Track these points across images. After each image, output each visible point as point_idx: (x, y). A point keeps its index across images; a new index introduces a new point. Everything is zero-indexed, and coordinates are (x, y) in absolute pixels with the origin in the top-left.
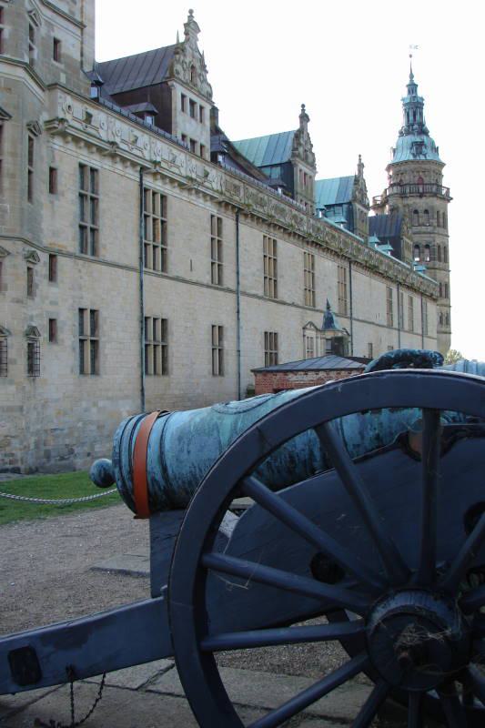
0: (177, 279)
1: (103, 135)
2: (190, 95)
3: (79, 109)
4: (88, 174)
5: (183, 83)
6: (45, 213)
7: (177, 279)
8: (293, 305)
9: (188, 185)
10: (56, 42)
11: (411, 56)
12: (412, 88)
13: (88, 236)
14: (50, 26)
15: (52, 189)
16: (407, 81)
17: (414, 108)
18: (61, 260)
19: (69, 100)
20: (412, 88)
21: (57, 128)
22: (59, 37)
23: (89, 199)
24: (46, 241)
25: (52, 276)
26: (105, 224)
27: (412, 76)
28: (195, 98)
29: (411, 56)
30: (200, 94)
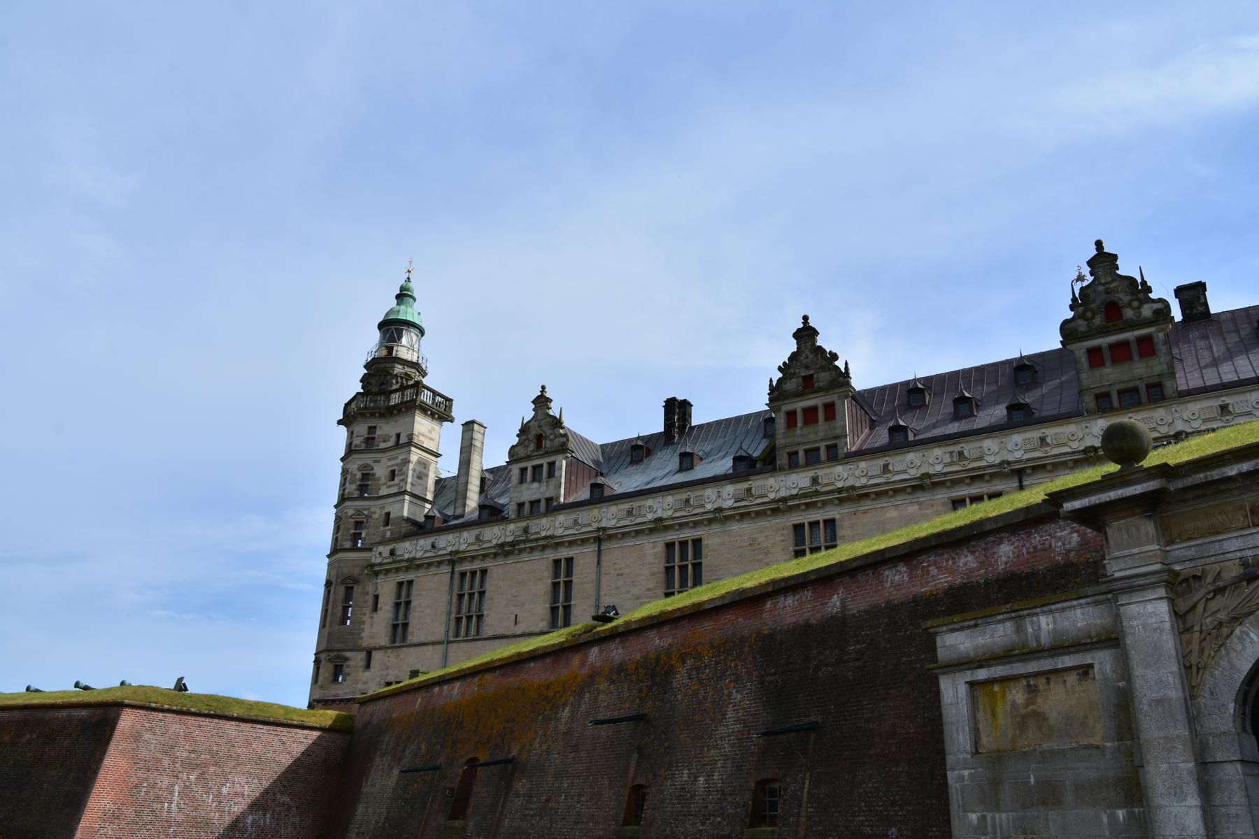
0: (495, 637)
2: (529, 465)
6: (366, 627)
7: (495, 637)
9: (506, 550)
10: (388, 514)
13: (399, 630)
14: (383, 508)
15: (375, 609)
18: (374, 653)
19: (381, 549)
23: (403, 605)
24: (365, 644)
26: (415, 619)
30: (547, 454)
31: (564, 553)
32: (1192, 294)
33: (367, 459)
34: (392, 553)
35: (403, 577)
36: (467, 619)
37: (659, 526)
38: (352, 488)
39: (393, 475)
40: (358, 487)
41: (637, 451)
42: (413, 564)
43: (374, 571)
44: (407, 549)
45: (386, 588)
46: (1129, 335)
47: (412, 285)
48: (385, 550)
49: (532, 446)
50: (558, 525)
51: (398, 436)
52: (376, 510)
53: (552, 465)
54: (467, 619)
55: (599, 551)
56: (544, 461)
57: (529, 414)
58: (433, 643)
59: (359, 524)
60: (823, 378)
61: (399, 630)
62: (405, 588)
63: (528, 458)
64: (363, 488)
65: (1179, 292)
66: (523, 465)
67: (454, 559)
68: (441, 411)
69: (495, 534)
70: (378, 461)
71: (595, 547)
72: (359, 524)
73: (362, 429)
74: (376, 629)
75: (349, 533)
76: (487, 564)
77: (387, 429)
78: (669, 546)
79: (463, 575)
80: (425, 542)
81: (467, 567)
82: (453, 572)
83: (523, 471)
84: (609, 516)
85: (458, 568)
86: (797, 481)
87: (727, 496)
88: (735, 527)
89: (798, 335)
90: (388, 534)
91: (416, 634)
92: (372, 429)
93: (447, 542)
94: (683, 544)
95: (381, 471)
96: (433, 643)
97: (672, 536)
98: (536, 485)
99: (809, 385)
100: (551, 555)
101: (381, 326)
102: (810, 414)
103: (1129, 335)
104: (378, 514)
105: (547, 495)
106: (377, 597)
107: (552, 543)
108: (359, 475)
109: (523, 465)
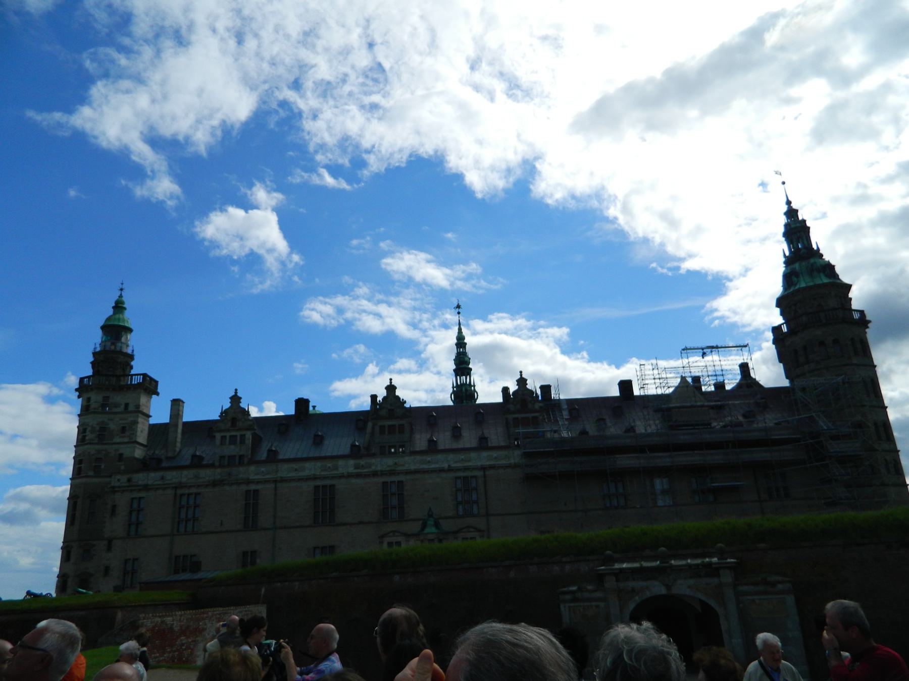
1: (140, 483)
2: (228, 434)
3: (124, 478)
5: (220, 431)
8: (361, 523)
9: (214, 484)
12: (791, 213)
16: (785, 208)
19: (119, 477)
20: (791, 213)
21: (114, 490)
22: (121, 452)
25: (109, 548)
27: (789, 203)
28: (233, 433)
29: (784, 183)
31: (253, 487)
32: (546, 389)
34: (129, 480)
37: (315, 478)
39: (123, 430)
42: (146, 488)
43: (114, 490)
44: (141, 478)
45: (122, 500)
46: (530, 415)
47: (124, 299)
49: (229, 424)
50: (251, 472)
51: (127, 405)
53: (243, 436)
55: (276, 489)
56: (238, 434)
57: (227, 405)
58: (162, 536)
63: (228, 430)
65: (542, 387)
66: (223, 434)
70: (111, 420)
71: (273, 485)
78: (317, 487)
79: (181, 495)
81: (187, 491)
82: (176, 494)
83: (223, 438)
84: (285, 471)
85: (179, 492)
86: (388, 462)
87: (349, 466)
88: (354, 481)
89: (388, 388)
90: (123, 467)
92: (106, 398)
94: (324, 487)
96: (162, 536)
97: (318, 483)
98: (232, 447)
99: (391, 415)
100: (244, 488)
101: (103, 328)
102: (392, 427)
103: (530, 415)
105: (241, 453)
106: (114, 507)
107: (248, 482)
108: (98, 428)
109: (223, 434)
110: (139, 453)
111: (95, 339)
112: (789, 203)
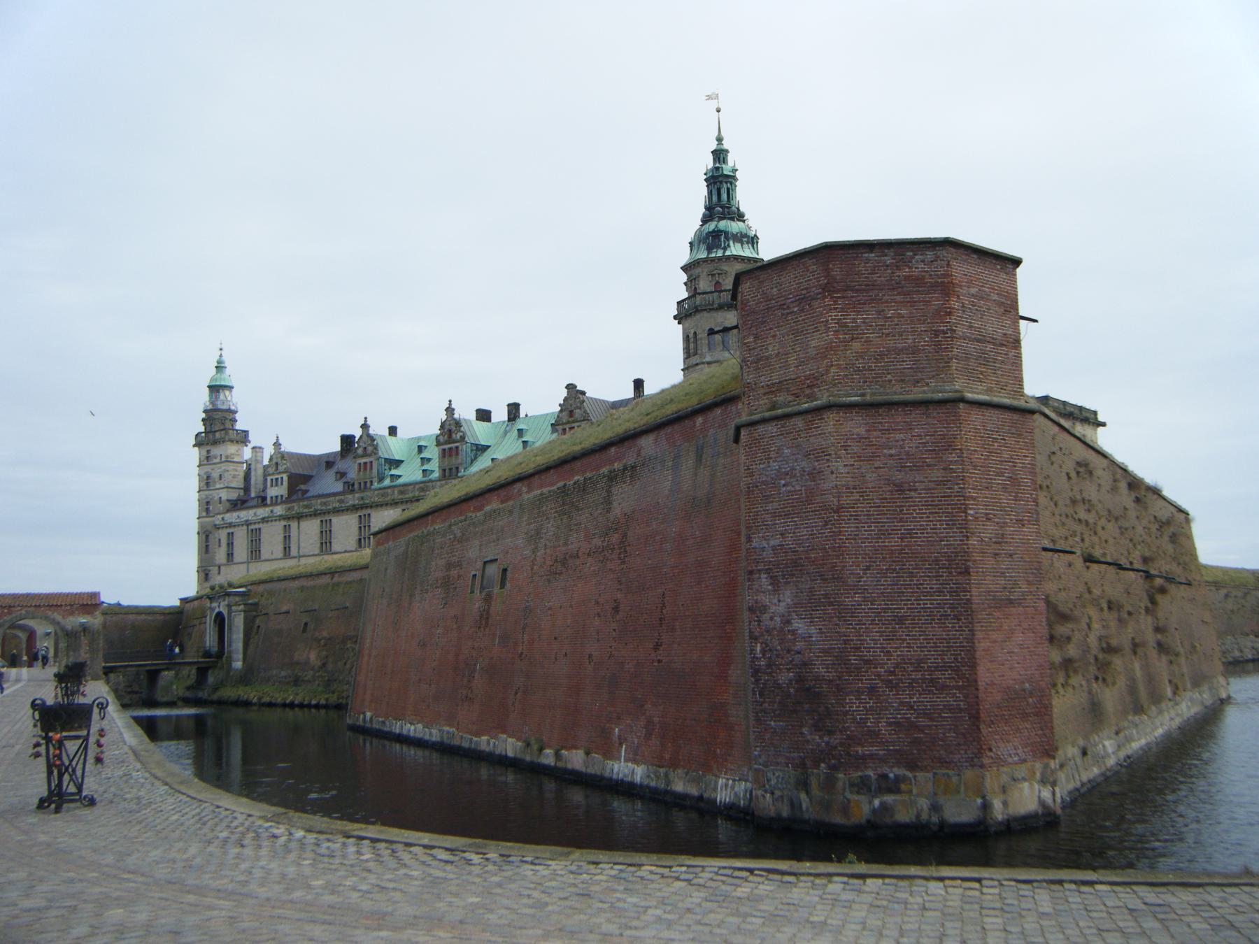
4: (230, 535)
9: (264, 520)
11: (718, 111)
12: (719, 155)
13: (230, 556)
17: (720, 182)
20: (719, 155)
23: (230, 544)
27: (720, 139)
33: (207, 468)
35: (230, 530)
36: (255, 553)
38: (203, 484)
40: (207, 482)
41: (328, 462)
42: (231, 525)
43: (217, 527)
45: (223, 534)
48: (220, 517)
52: (216, 495)
54: (255, 553)
59: (208, 503)
60: (370, 449)
61: (230, 556)
62: (230, 535)
64: (207, 484)
67: (247, 523)
68: (243, 437)
69: (262, 512)
72: (208, 503)
73: (204, 452)
74: (220, 555)
75: (206, 507)
76: (261, 525)
77: (217, 451)
80: (235, 514)
81: (253, 527)
91: (237, 558)
92: (208, 452)
93: (245, 515)
95: (215, 475)
104: (216, 498)
110: (234, 495)
111: (204, 397)
112: (720, 139)
